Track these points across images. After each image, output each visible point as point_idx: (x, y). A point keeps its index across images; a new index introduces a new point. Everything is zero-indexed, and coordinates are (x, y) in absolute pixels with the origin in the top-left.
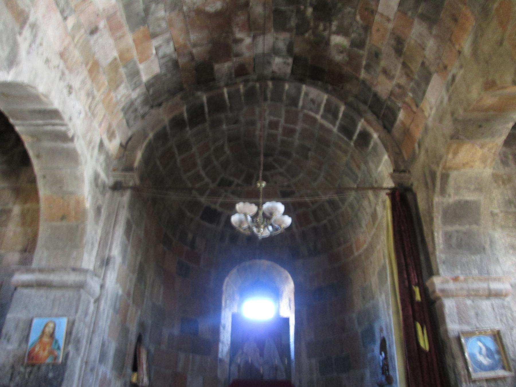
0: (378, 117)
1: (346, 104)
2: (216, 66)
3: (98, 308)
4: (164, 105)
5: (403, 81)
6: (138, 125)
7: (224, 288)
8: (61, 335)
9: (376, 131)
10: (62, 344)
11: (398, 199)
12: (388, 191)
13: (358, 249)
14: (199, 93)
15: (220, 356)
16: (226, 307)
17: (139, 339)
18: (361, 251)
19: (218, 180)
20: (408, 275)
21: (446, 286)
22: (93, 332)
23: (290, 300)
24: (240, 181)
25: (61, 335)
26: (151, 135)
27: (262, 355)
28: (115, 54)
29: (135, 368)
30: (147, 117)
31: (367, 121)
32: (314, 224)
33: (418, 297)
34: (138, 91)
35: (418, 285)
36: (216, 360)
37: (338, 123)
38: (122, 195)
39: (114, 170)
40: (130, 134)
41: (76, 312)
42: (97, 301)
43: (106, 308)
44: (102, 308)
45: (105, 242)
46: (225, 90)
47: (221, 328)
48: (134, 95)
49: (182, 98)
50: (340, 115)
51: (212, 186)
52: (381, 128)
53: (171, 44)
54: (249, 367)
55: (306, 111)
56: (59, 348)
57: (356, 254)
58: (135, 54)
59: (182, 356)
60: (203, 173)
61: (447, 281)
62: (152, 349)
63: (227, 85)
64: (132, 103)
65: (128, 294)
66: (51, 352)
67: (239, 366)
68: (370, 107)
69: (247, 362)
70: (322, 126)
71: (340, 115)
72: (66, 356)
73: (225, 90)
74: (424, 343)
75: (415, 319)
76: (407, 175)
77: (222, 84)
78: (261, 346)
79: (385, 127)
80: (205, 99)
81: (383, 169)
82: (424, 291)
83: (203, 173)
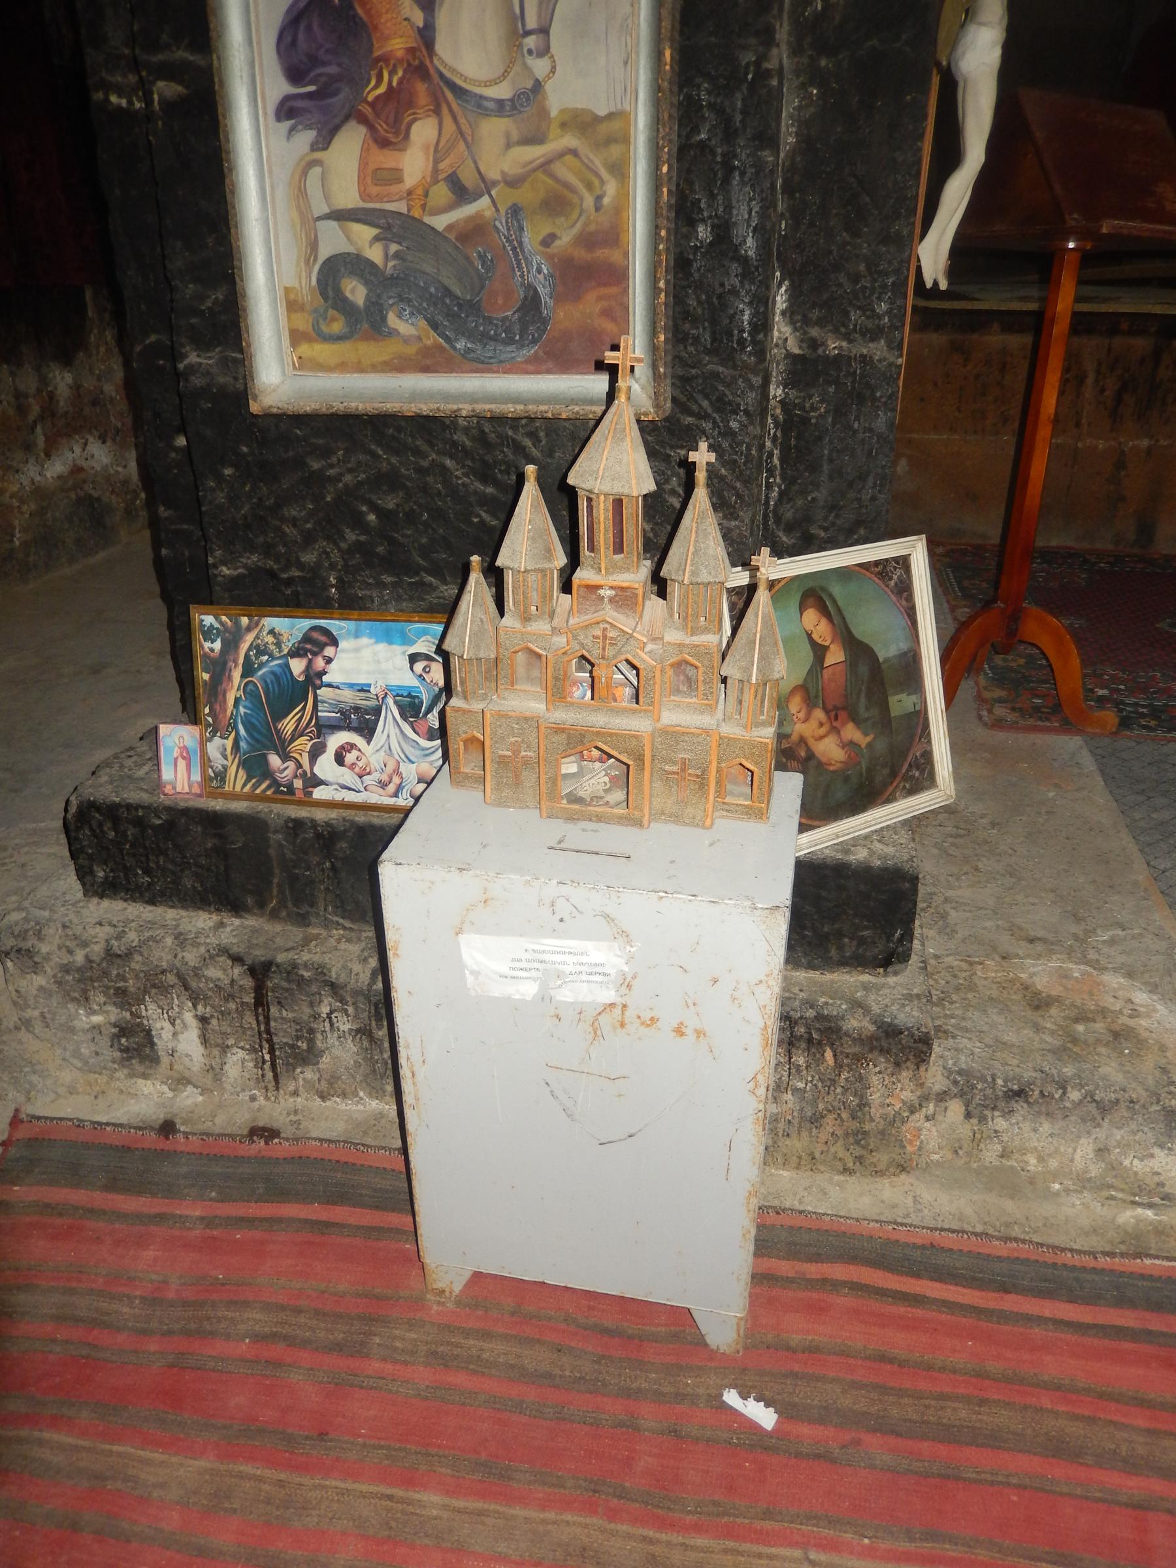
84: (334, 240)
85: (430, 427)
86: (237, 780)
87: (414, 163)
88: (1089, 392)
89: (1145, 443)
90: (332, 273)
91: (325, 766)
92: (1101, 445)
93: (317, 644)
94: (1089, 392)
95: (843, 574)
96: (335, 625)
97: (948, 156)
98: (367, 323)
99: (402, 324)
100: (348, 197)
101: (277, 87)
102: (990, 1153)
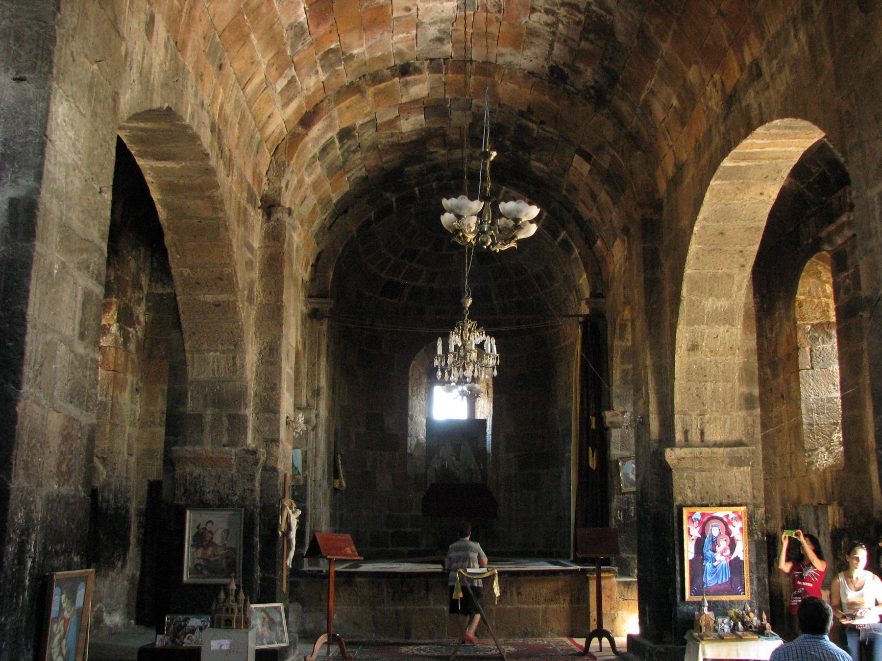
2: (406, 169)
3: (316, 435)
4: (350, 211)
5: (598, 219)
7: (410, 374)
10: (300, 469)
12: (581, 319)
14: (388, 195)
15: (409, 451)
16: (413, 395)
17: (335, 446)
18: (566, 343)
21: (615, 419)
22: (316, 456)
27: (458, 459)
29: (336, 475)
31: (570, 234)
33: (593, 426)
36: (406, 456)
38: (322, 324)
39: (310, 296)
44: (320, 435)
46: (416, 189)
48: (324, 217)
53: (364, 170)
56: (299, 474)
57: (563, 344)
61: (617, 415)
63: (417, 184)
65: (329, 413)
69: (443, 466)
72: (306, 479)
74: (593, 463)
76: (602, 300)
77: (413, 182)
80: (394, 199)
81: (583, 281)
82: (600, 420)
84: (197, 561)
85: (207, 586)
86: (170, 644)
87: (209, 552)
88: (385, 593)
89: (403, 608)
94: (385, 593)
95: (269, 608)
97: (290, 548)
98: (201, 572)
99: (206, 572)
100: (199, 556)
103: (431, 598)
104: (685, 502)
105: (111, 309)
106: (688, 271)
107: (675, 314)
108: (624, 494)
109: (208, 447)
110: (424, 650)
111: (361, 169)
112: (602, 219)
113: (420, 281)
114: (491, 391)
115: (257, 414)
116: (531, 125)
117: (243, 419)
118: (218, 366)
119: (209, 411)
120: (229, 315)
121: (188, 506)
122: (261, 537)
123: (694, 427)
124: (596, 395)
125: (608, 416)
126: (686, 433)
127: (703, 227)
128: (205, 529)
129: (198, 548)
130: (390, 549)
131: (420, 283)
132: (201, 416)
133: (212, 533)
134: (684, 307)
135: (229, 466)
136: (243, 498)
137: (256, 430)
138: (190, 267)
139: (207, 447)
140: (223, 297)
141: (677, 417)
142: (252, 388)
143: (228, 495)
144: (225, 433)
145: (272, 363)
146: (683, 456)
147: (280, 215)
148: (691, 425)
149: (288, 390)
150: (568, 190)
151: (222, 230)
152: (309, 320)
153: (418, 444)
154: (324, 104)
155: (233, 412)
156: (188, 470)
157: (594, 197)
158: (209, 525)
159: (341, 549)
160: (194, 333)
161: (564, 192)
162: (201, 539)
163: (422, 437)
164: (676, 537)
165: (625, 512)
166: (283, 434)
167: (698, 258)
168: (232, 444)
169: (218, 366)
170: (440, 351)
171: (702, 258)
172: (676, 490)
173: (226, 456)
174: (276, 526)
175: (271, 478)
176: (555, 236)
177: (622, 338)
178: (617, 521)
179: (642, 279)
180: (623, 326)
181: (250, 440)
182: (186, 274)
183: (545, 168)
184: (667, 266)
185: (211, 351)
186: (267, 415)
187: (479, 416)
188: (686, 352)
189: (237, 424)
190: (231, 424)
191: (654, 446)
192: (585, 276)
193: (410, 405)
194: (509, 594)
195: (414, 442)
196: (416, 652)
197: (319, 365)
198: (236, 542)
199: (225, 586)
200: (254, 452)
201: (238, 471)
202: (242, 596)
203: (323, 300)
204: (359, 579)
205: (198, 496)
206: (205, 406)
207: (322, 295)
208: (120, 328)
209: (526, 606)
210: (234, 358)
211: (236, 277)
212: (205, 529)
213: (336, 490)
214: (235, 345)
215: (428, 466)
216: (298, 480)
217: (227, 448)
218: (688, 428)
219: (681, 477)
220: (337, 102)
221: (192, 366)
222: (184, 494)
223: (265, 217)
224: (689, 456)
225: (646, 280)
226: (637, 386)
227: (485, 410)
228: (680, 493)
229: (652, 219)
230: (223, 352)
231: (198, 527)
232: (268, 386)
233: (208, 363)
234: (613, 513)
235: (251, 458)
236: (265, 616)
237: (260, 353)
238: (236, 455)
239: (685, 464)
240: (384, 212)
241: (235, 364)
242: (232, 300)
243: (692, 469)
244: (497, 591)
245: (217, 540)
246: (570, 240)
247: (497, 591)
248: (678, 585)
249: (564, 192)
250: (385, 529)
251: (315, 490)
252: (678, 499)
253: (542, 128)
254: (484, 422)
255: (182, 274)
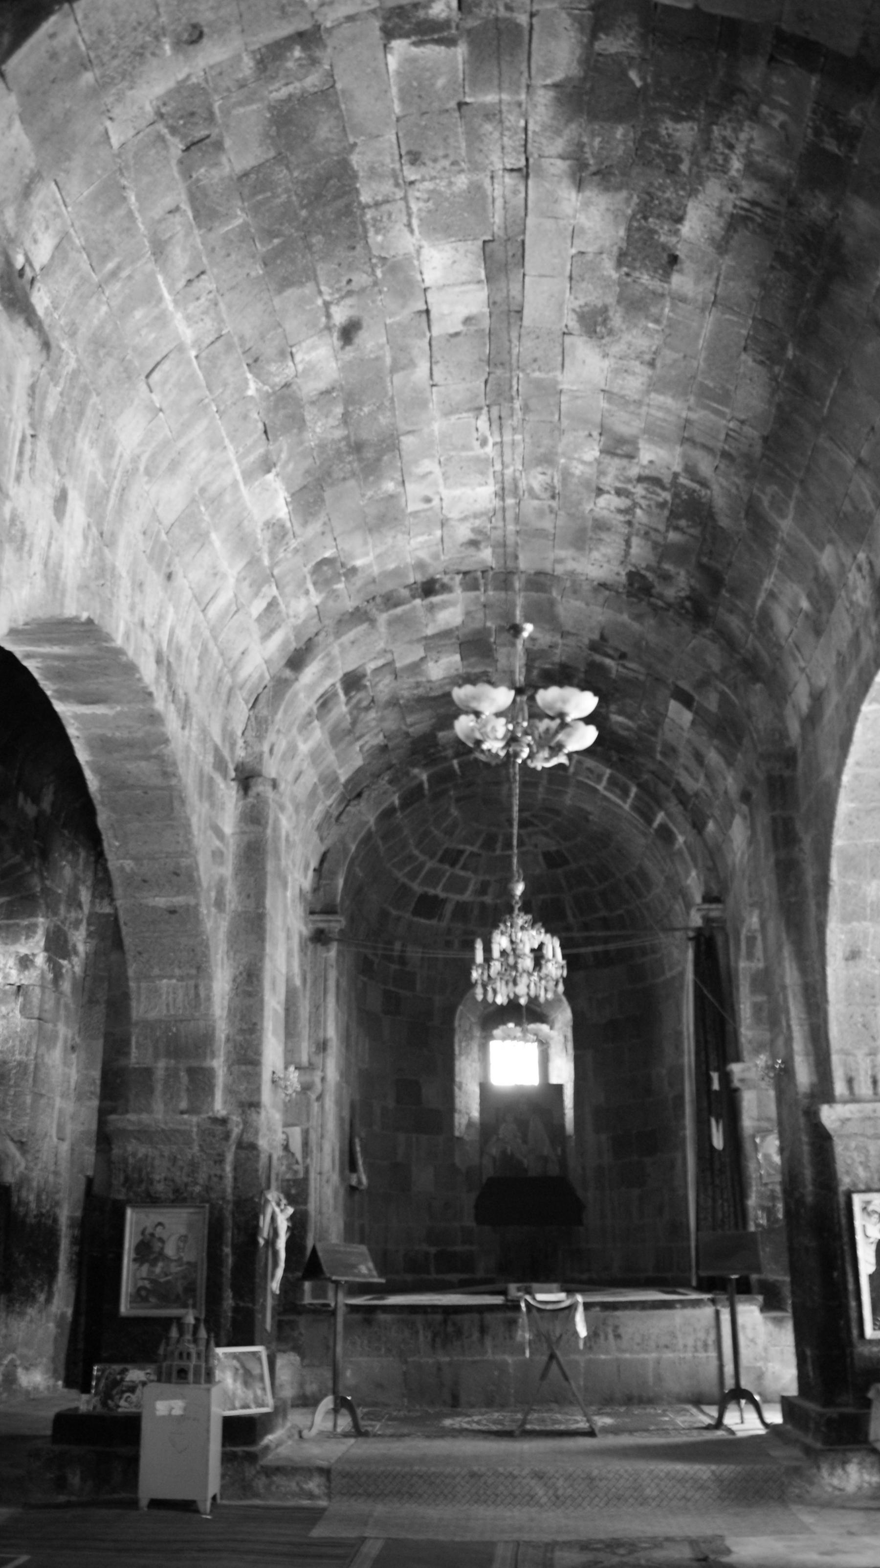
0: (685, 809)
1: (639, 785)
3: (322, 1107)
4: (365, 795)
5: (708, 790)
6: (333, 834)
7: (456, 1023)
8: (296, 1146)
9: (683, 833)
10: (299, 1156)
11: (703, 947)
13: (671, 969)
14: (416, 771)
15: (457, 1134)
17: (352, 1125)
19: (440, 853)
20: (707, 1057)
21: (747, 1075)
22: (322, 1137)
23: (565, 1037)
24: (475, 849)
25: (296, 1146)
26: (353, 848)
27: (525, 1142)
28: (315, 780)
29: (353, 1166)
30: (344, 818)
31: (669, 815)
32: (603, 913)
33: (716, 1086)
34: (335, 795)
35: (717, 1069)
36: (454, 1141)
37: (629, 801)
38: (328, 951)
39: (312, 913)
40: (323, 849)
41: (308, 1120)
42: (320, 1098)
43: (330, 1103)
45: (316, 1021)
46: (455, 763)
47: (456, 1090)
48: (329, 802)
49: (390, 782)
50: (632, 795)
51: (429, 865)
52: (689, 827)
53: (381, 736)
54: (508, 1160)
55: (580, 778)
57: (668, 975)
58: (336, 765)
59: (402, 1137)
60: (416, 852)
62: (363, 1134)
64: (327, 812)
65: (342, 1075)
66: (289, 1167)
67: (494, 1158)
68: (674, 791)
69: (504, 1152)
70: (605, 798)
71: (632, 795)
72: (307, 1170)
73: (455, 763)
74: (718, 1142)
75: (710, 1113)
78: (522, 1125)
79: (694, 825)
80: (424, 777)
82: (726, 1078)
83: (416, 852)
84: (140, 1283)
87: (158, 1270)
89: (447, 1359)
90: (139, 1289)
91: (122, 1403)
92: (431, 1361)
93: (124, 1371)
94: (421, 1338)
95: (244, 1353)
96: (128, 1366)
97: (276, 1265)
98: (145, 1299)
99: (153, 1300)
100: (144, 1275)
101: (133, 1255)
102: (273, 1488)
103: (488, 1342)
104: (855, 1185)
105: (35, 932)
106: (838, 842)
107: (823, 906)
108: (766, 1184)
109: (160, 1116)
110: (478, 1423)
111: (377, 735)
112: (714, 790)
113: (468, 893)
114: (570, 1045)
115: (229, 1068)
116: (608, 661)
117: (209, 1073)
118: (175, 1000)
119: (161, 1064)
120: (189, 926)
121: (129, 1202)
122: (234, 1247)
123: (862, 1073)
124: (718, 1041)
125: (736, 1068)
126: (850, 1081)
127: (856, 777)
128: (152, 1235)
129: (142, 1264)
130: (434, 1276)
131: (467, 896)
132: (148, 1072)
133: (161, 1240)
134: (835, 896)
135: (189, 1143)
136: (208, 1189)
137: (229, 1091)
138: (135, 859)
139: (158, 1113)
140: (180, 900)
141: (835, 1059)
142: (222, 1030)
143: (186, 1185)
144: (183, 1094)
145: (250, 995)
146: (848, 1115)
147: (260, 788)
148: (857, 1070)
149: (275, 1033)
150: (664, 754)
151: (176, 804)
152: (311, 946)
153: (470, 1124)
154: (320, 638)
155: (194, 1063)
156: (130, 1148)
157: (699, 758)
158: (159, 1229)
159: (354, 1266)
160: (140, 953)
161: (659, 757)
162: (146, 1250)
163: (475, 1114)
164: (846, 1239)
165: (770, 1212)
166: (267, 1095)
167: (851, 823)
168: (193, 1110)
169: (175, 1000)
170: (479, 957)
171: (857, 822)
172: (840, 1166)
173: (183, 1128)
174: (255, 1230)
175: (248, 1159)
176: (649, 821)
177: (750, 956)
178: (758, 1225)
179: (772, 860)
180: (751, 940)
181: (219, 1105)
182: (128, 869)
183: (630, 724)
184: (807, 841)
185: (164, 977)
186: (243, 1068)
187: (554, 1080)
188: (843, 963)
189: (200, 1082)
190: (192, 1080)
191: (805, 1102)
192: (694, 873)
193: (457, 1069)
194: (602, 1337)
195: (464, 1121)
196: (466, 1426)
197: (326, 1007)
198: (195, 1254)
199: (179, 1320)
200: (224, 1121)
201: (202, 1149)
202: (203, 1333)
203: (330, 918)
204: (382, 1317)
205: (143, 1187)
206: (156, 1057)
207: (329, 910)
208: (49, 960)
209: (627, 1356)
210: (196, 987)
211: (197, 869)
212: (152, 1235)
213: (352, 1190)
214: (198, 968)
215: (482, 1153)
216: (296, 1172)
217: (186, 1116)
218: (853, 1074)
219: (846, 1148)
220: (338, 635)
221: (138, 1000)
222: (124, 1185)
223: (241, 792)
224: (857, 1115)
225: (778, 863)
226: (772, 1017)
227: (563, 1072)
228: (848, 1173)
229: (781, 777)
230: (181, 979)
231: (143, 1233)
232: (245, 1027)
233: (160, 996)
234: (751, 1214)
235: (219, 1129)
236: (238, 1365)
237: (234, 980)
238: (198, 1126)
239: (851, 1128)
240: (412, 796)
241: (197, 995)
242: (193, 902)
243: (863, 1135)
244: (582, 1330)
245: (170, 1250)
246: (671, 825)
247: (582, 1330)
248: (854, 1314)
249: (659, 757)
250: (425, 1247)
251: (321, 1187)
252: (845, 1182)
253: (624, 667)
254: (559, 1088)
255: (122, 869)
